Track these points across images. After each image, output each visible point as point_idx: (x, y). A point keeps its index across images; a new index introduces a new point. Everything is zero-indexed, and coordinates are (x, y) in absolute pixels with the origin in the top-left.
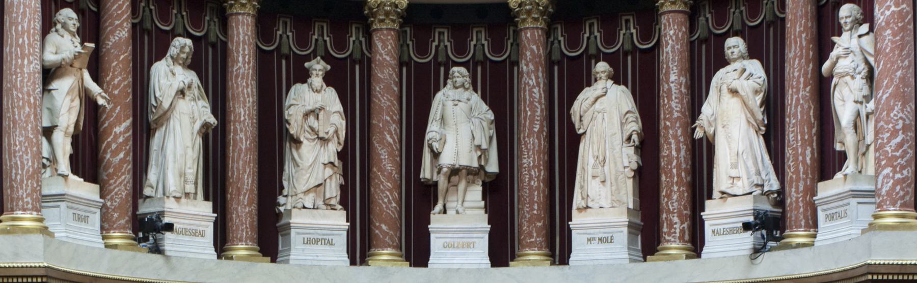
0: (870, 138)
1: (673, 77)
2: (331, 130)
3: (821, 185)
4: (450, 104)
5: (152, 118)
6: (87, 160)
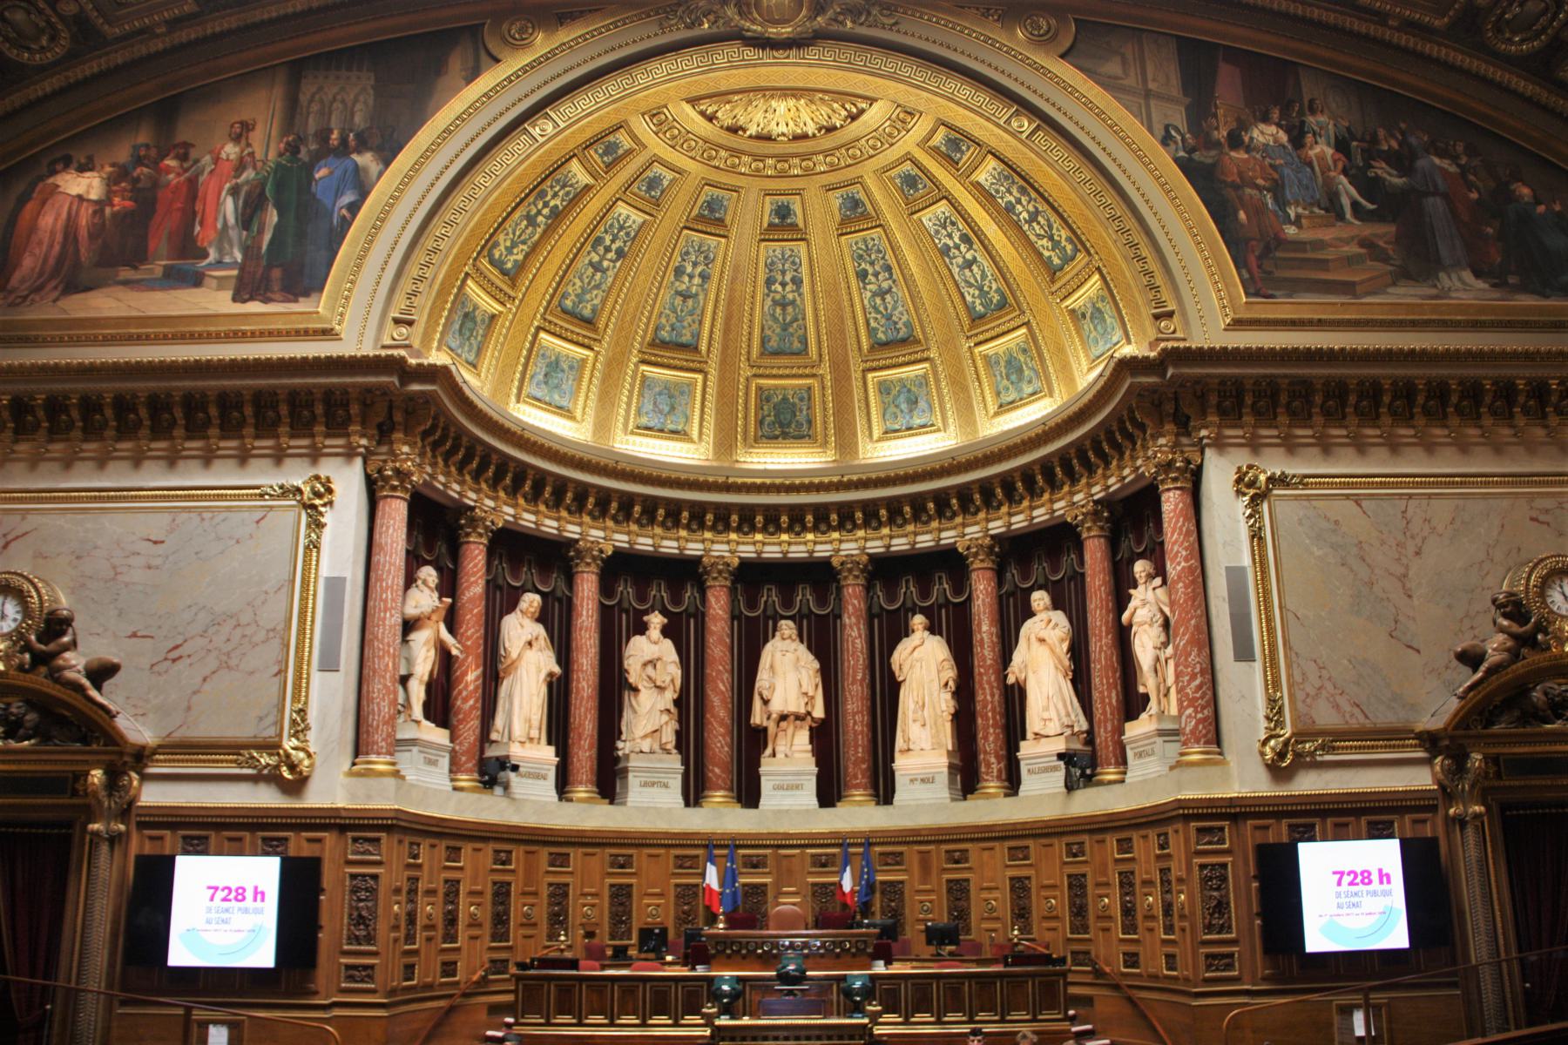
0: (1171, 679)
1: (985, 628)
2: (668, 679)
3: (1128, 725)
4: (778, 655)
5: (501, 667)
6: (440, 707)
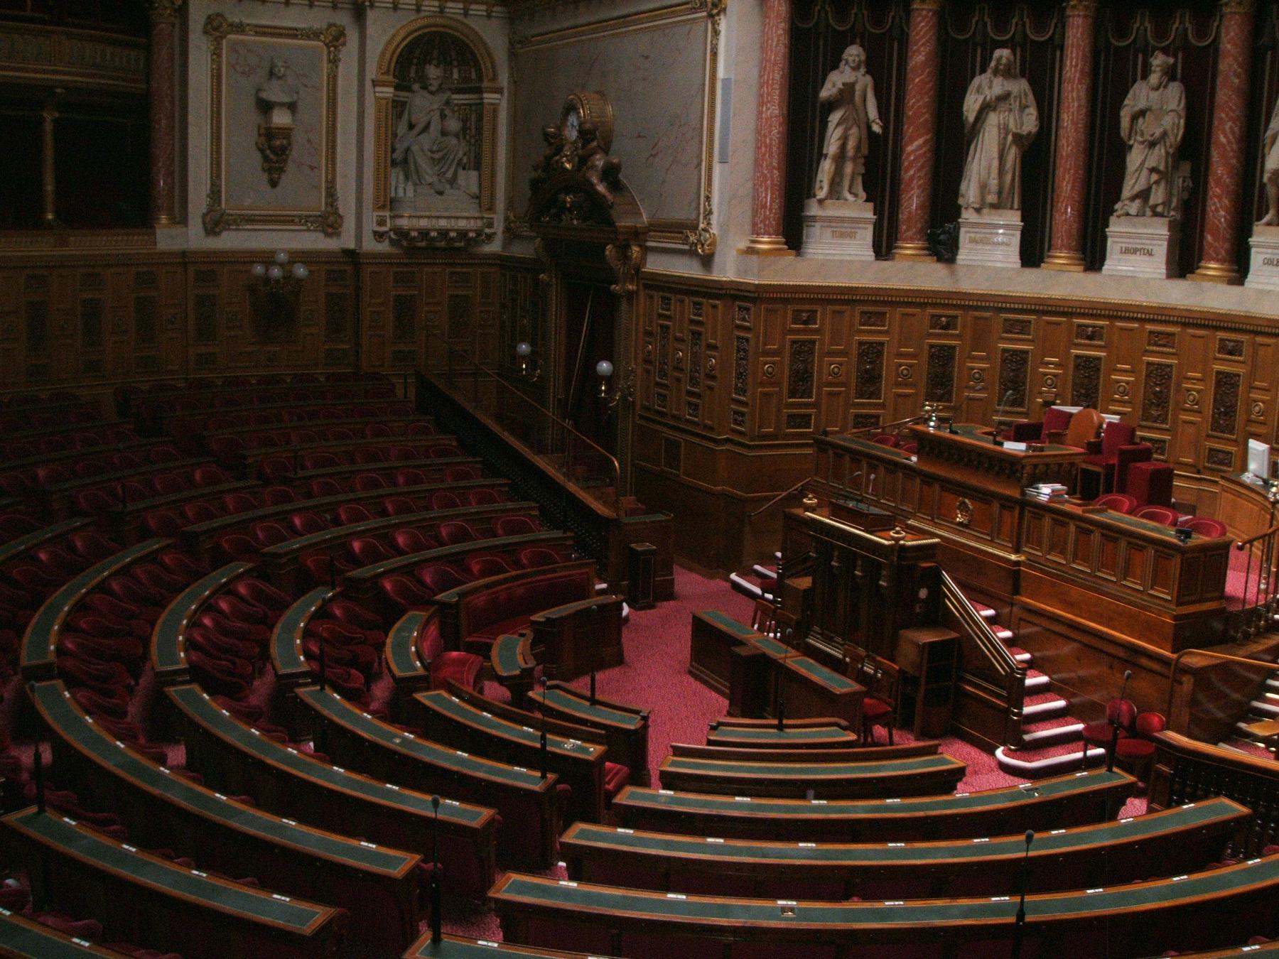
2: (1158, 133)
